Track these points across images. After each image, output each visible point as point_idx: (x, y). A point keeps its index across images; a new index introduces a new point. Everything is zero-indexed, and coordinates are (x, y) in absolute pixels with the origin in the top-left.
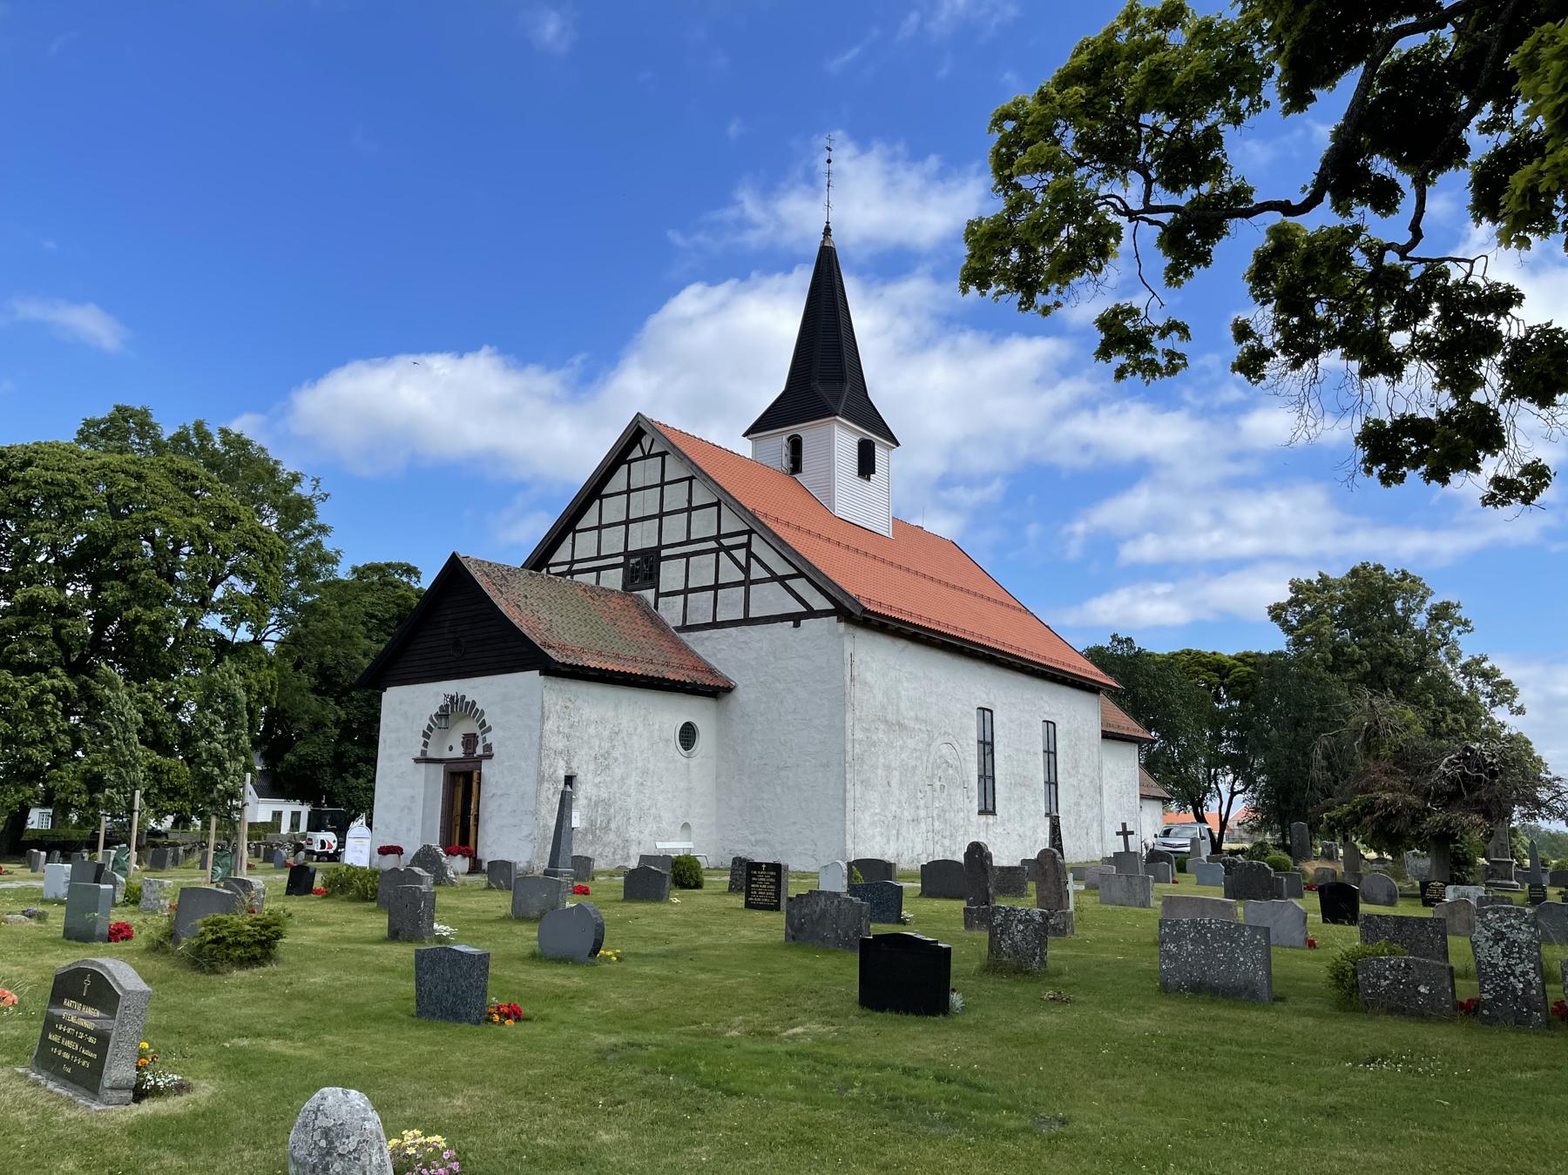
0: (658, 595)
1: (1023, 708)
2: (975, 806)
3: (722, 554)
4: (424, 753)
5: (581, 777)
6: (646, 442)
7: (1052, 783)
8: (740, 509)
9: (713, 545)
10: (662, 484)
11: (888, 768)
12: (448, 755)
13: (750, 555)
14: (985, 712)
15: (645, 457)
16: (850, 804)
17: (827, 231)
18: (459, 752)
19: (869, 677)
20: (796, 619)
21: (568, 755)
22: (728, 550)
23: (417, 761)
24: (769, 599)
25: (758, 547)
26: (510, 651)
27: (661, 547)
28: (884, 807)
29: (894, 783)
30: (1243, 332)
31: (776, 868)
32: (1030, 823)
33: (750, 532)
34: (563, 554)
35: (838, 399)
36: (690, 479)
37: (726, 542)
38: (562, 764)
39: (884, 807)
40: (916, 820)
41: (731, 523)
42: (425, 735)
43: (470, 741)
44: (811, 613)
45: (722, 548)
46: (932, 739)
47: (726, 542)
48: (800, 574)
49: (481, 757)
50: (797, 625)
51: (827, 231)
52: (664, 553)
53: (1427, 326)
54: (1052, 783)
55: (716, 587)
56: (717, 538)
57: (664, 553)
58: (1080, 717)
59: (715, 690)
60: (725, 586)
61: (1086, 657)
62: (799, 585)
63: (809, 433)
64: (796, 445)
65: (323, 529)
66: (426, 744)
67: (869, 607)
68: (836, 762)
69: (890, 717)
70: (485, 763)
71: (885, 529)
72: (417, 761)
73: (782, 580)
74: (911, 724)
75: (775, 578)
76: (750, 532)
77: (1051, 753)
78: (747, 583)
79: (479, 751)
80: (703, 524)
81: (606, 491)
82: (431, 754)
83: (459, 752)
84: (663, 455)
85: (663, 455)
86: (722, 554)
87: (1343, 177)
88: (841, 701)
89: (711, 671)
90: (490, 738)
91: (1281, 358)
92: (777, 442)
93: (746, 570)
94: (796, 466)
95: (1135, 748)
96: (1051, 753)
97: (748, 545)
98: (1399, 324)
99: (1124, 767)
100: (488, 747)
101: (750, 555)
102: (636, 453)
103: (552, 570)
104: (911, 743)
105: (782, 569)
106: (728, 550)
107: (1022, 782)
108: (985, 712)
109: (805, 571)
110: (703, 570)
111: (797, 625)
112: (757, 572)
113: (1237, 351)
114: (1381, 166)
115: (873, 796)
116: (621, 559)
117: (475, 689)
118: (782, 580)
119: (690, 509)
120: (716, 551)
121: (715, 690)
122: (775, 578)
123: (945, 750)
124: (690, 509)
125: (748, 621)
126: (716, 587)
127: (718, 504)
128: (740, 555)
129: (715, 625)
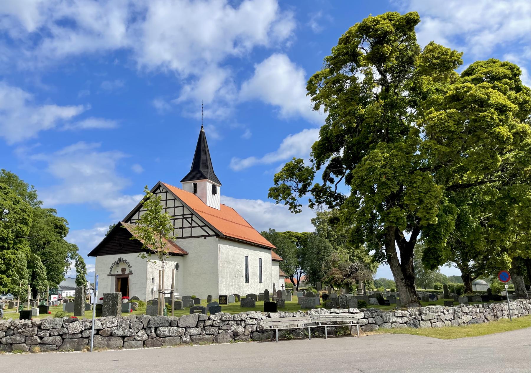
1: (254, 255)
2: (244, 281)
3: (184, 220)
4: (110, 273)
5: (155, 278)
6: (161, 188)
7: (261, 274)
8: (189, 208)
9: (182, 217)
10: (166, 200)
11: (227, 273)
12: (116, 273)
13: (192, 220)
14: (247, 257)
16: (219, 282)
18: (120, 272)
19: (223, 251)
20: (205, 237)
21: (152, 273)
22: (186, 218)
23: (108, 275)
24: (198, 231)
25: (194, 218)
26: (136, 247)
28: (226, 282)
29: (228, 276)
30: (310, 201)
31: (226, 296)
32: (256, 285)
33: (192, 214)
34: (136, 217)
35: (207, 174)
36: (175, 199)
37: (185, 216)
38: (151, 275)
39: (226, 282)
40: (232, 285)
41: (186, 212)
42: (110, 268)
43: (124, 270)
44: (209, 235)
45: (184, 218)
46: (236, 265)
47: (185, 216)
48: (206, 226)
49: (128, 274)
50: (205, 238)
53: (338, 201)
54: (261, 274)
55: (183, 228)
56: (183, 215)
58: (267, 257)
59: (183, 255)
60: (185, 228)
61: (262, 235)
62: (206, 228)
63: (199, 183)
64: (195, 186)
65: (41, 202)
66: (111, 271)
67: (225, 234)
68: (215, 273)
69: (227, 260)
70: (130, 276)
71: (218, 207)
72: (108, 275)
73: (201, 227)
74: (231, 262)
75: (199, 226)
76: (192, 214)
77: (260, 266)
78: (192, 227)
79: (127, 272)
80: (179, 211)
82: (112, 273)
83: (120, 272)
84: (166, 192)
85: (166, 192)
86: (184, 220)
87: (326, 177)
88: (216, 258)
89: (182, 250)
90: (131, 269)
91: (317, 204)
92: (190, 185)
93: (191, 224)
94: (195, 191)
95: (278, 263)
96: (260, 266)
97: (192, 218)
98: (334, 201)
99: (276, 268)
100: (131, 272)
101: (192, 220)
102: (158, 191)
103: (132, 221)
104: (231, 266)
105: (201, 224)
106: (186, 218)
107: (254, 274)
108: (247, 257)
109: (207, 225)
110: (179, 223)
111: (205, 238)
112: (194, 224)
113: (309, 204)
114: (332, 175)
115: (224, 280)
118: (201, 227)
119: (175, 207)
120: (183, 219)
121: (183, 255)
122: (199, 226)
123: (238, 267)
124: (175, 207)
125: (191, 237)
126: (183, 228)
127: (183, 206)
128: (190, 220)
129: (182, 238)
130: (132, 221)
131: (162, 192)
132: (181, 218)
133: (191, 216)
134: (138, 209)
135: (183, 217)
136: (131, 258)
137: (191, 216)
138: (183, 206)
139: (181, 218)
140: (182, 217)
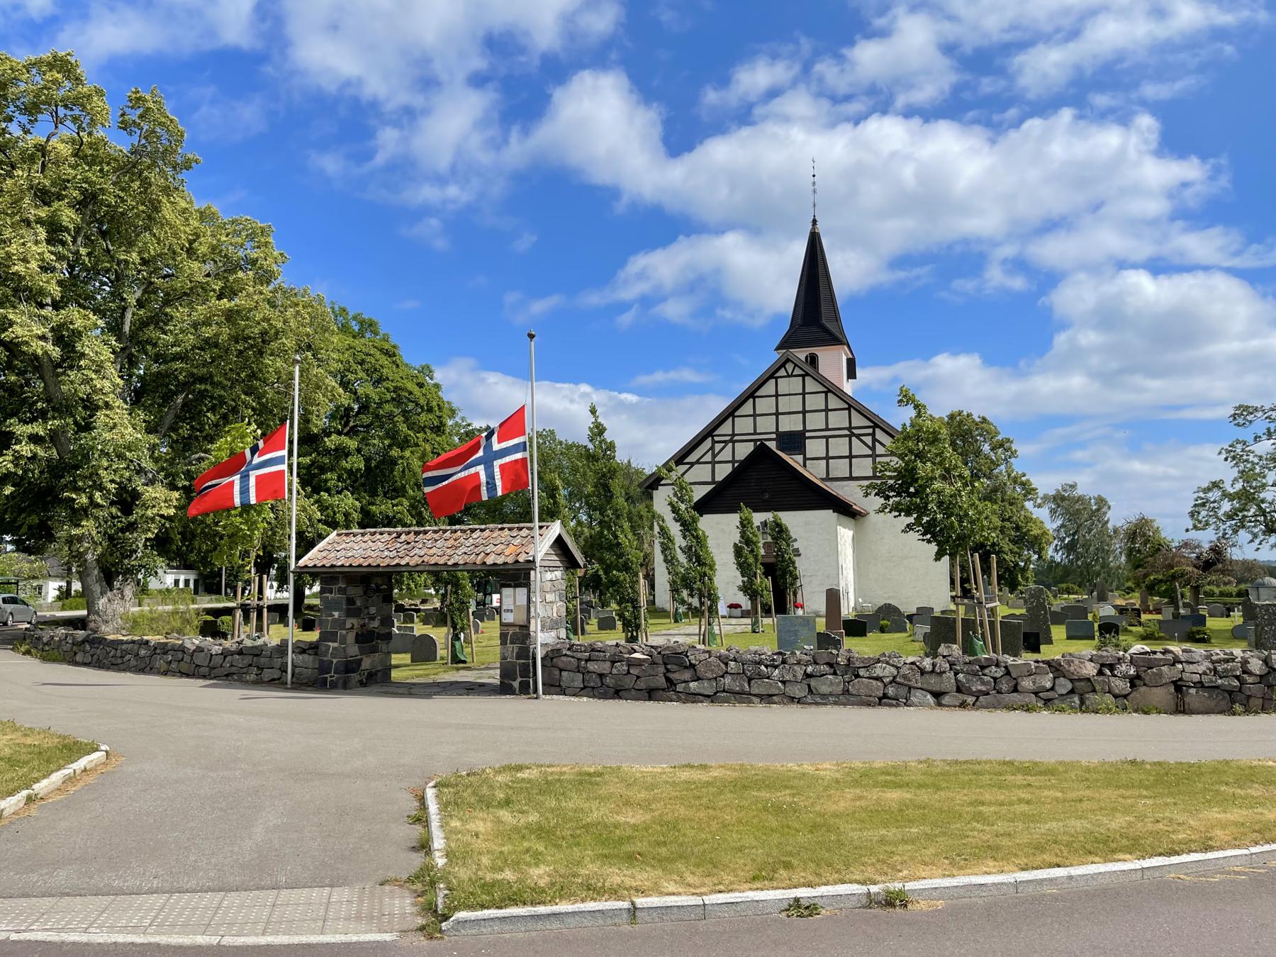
0: (805, 459)
9: (847, 432)
13: (874, 440)
15: (788, 376)
17: (814, 222)
22: (858, 436)
27: (805, 431)
37: (855, 431)
41: (858, 420)
45: (853, 434)
47: (855, 431)
51: (814, 222)
56: (850, 428)
57: (808, 434)
60: (856, 457)
81: (757, 394)
93: (873, 448)
97: (873, 434)
101: (874, 440)
102: (782, 372)
103: (716, 439)
106: (858, 436)
110: (839, 446)
112: (880, 450)
116: (774, 436)
117: (790, 519)
124: (827, 410)
128: (868, 440)
130: (716, 439)
131: (792, 376)
132: (845, 436)
133: (870, 431)
135: (851, 433)
136: (796, 521)
137: (870, 431)
138: (849, 409)
139: (845, 436)
140: (847, 432)
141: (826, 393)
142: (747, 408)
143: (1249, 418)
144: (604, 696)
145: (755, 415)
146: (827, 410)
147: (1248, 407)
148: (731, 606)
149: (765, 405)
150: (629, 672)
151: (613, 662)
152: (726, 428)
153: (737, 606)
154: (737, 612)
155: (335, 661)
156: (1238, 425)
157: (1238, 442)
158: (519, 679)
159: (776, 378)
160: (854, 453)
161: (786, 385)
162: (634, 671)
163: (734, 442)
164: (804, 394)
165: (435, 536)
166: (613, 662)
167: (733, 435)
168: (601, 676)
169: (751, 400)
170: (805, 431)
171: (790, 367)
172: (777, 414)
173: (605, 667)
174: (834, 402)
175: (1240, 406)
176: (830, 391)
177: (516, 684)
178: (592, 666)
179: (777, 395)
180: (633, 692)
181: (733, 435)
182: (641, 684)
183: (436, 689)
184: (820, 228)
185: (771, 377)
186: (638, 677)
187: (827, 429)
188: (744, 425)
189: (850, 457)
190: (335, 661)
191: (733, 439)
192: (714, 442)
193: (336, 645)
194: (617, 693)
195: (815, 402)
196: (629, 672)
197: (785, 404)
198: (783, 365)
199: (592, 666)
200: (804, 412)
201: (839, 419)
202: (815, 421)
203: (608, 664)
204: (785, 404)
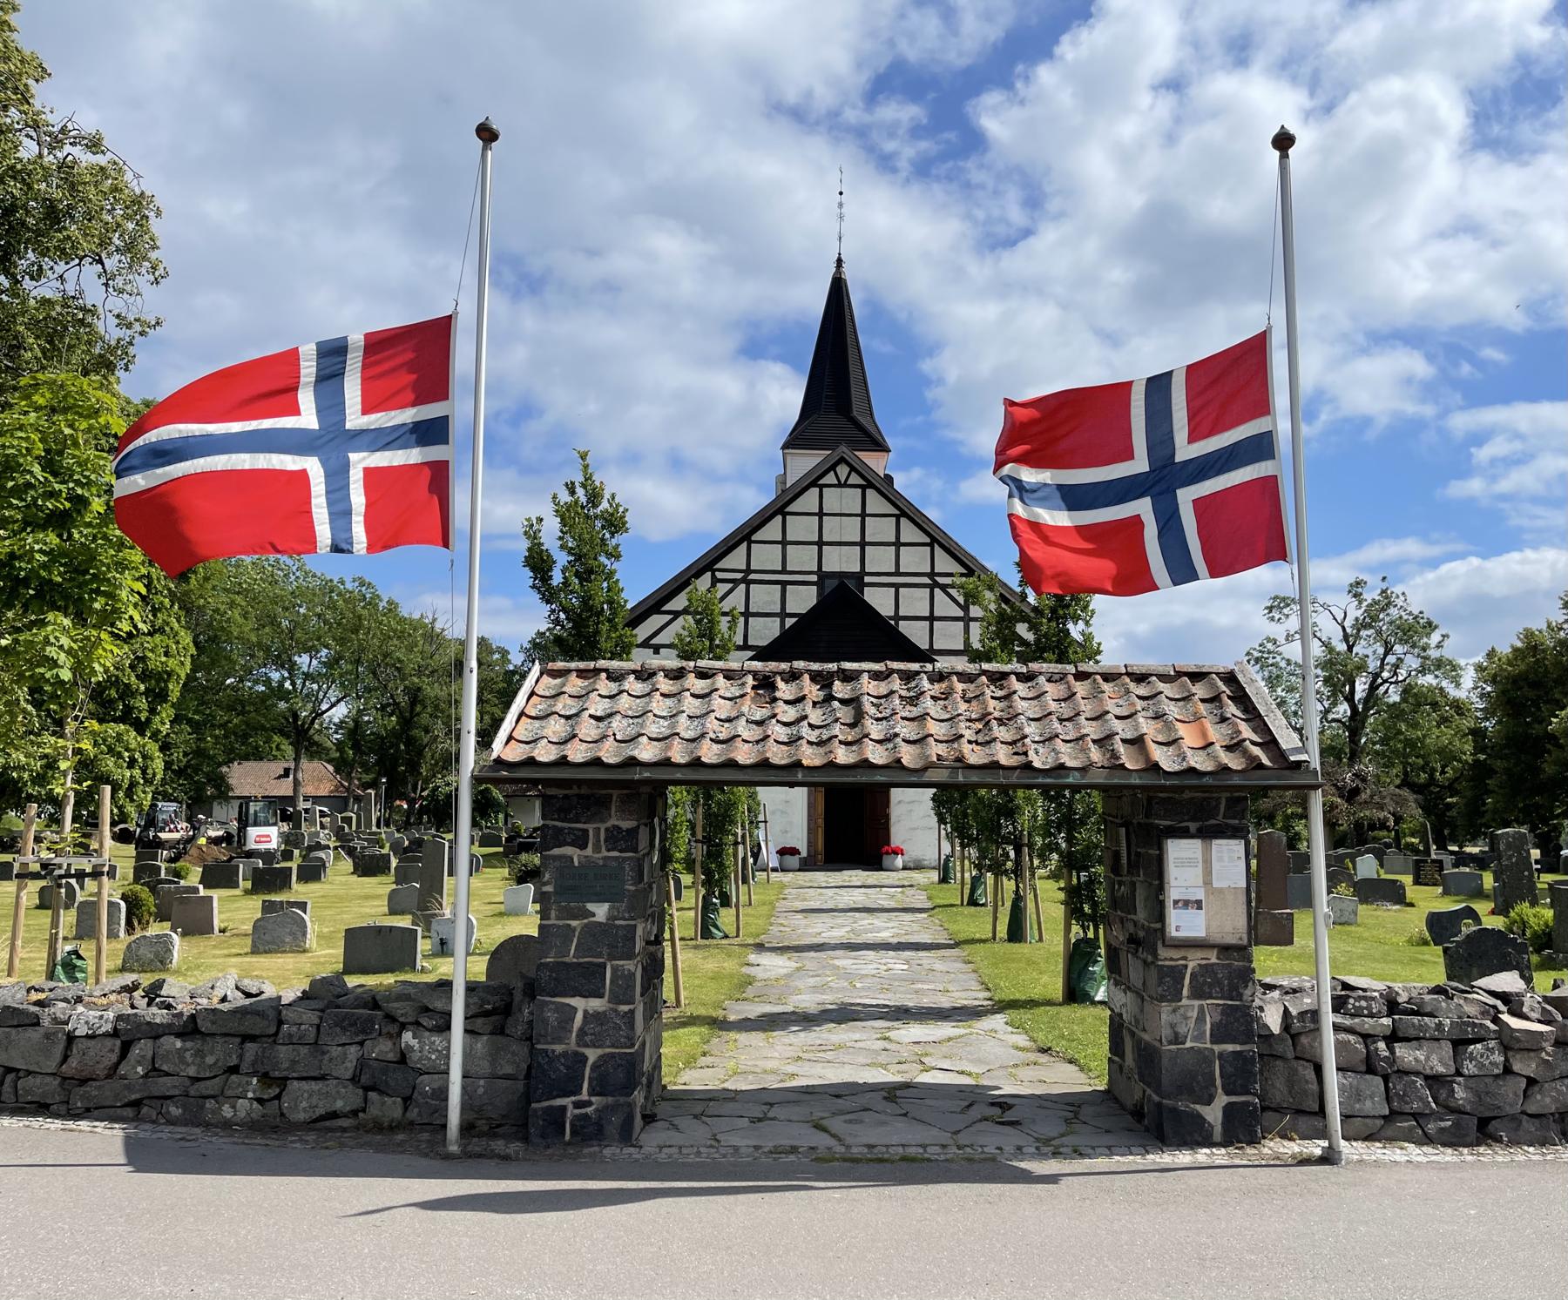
3: (937, 590)
9: (926, 580)
15: (840, 485)
22: (944, 588)
27: (863, 573)
37: (941, 580)
41: (944, 563)
52: (867, 579)
57: (867, 579)
81: (788, 509)
86: (937, 590)
93: (965, 608)
102: (830, 479)
103: (719, 575)
106: (944, 588)
116: (814, 578)
130: (719, 575)
131: (845, 485)
134: (745, 535)
135: (933, 582)
138: (931, 545)
140: (926, 580)
141: (898, 517)
142: (772, 530)
143: (1286, 611)
144: (1452, 1140)
145: (784, 543)
146: (898, 544)
147: (1284, 599)
148: (783, 852)
149: (802, 528)
150: (1508, 1070)
151: (1460, 1044)
152: (736, 560)
153: (793, 851)
154: (793, 861)
155: (592, 1055)
156: (1272, 619)
157: (1269, 640)
158: (1222, 1100)
159: (821, 487)
160: (901, 614)
161: (835, 499)
162: (1524, 1066)
163: (748, 583)
164: (863, 515)
165: (883, 688)
166: (1460, 1044)
167: (748, 571)
168: (1433, 1080)
169: (779, 518)
170: (863, 573)
171: (843, 471)
172: (820, 543)
173: (1437, 1060)
174: (909, 533)
175: (1275, 598)
176: (904, 514)
177: (1213, 1114)
178: (1407, 1055)
179: (821, 514)
180: (1529, 1126)
181: (748, 571)
182: (1544, 1101)
183: (895, 1135)
184: (847, 273)
185: (813, 484)
186: (1531, 1082)
187: (897, 573)
188: (765, 557)
189: (931, 618)
190: (592, 1055)
191: (747, 578)
192: (715, 581)
193: (595, 1004)
194: (1479, 1128)
195: (880, 529)
196: (1508, 1070)
197: (832, 528)
198: (833, 468)
199: (1407, 1055)
200: (863, 544)
201: (916, 560)
202: (881, 559)
203: (1447, 1048)
204: (832, 528)
